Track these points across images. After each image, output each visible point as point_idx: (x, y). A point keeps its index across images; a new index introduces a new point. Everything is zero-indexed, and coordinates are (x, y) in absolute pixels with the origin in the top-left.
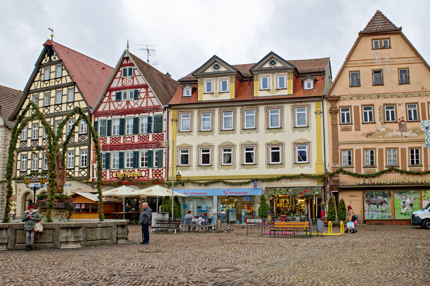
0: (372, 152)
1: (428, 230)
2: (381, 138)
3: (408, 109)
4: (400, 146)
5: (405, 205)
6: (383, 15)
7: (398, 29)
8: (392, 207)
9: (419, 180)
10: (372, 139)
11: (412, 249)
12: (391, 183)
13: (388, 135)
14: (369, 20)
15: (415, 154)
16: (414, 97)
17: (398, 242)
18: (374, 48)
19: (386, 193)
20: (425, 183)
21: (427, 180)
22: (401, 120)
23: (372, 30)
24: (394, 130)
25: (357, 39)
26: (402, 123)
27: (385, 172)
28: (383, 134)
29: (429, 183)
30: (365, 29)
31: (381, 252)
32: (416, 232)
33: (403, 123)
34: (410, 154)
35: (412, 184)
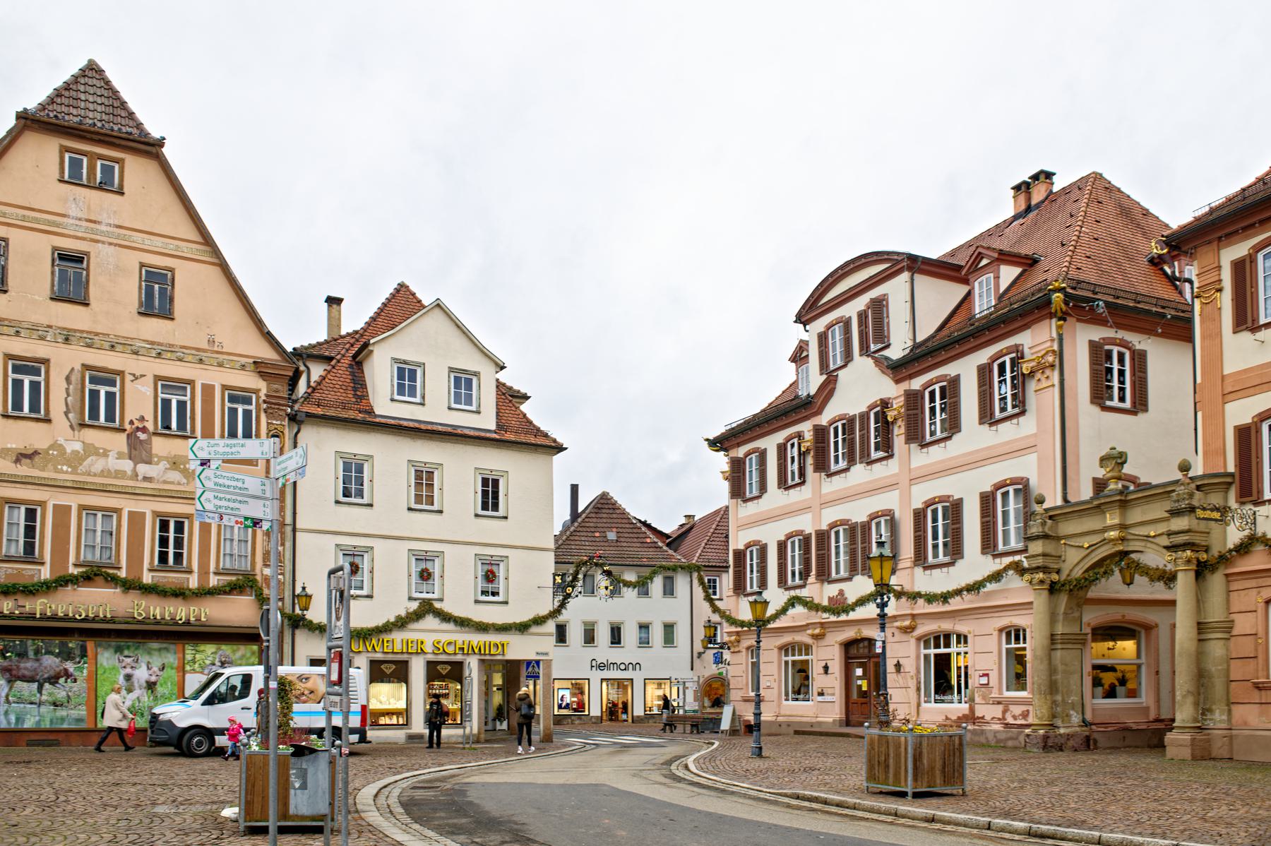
0: (31, 514)
1: (195, 760)
2: (67, 472)
3: (161, 396)
4: (128, 506)
5: (132, 685)
6: (108, 82)
7: (151, 141)
8: (89, 689)
9: (181, 611)
10: (36, 473)
11: (140, 816)
12: (91, 615)
13: (90, 466)
14: (59, 83)
15: (172, 535)
16: (183, 364)
17: (98, 796)
18: (66, 177)
19: (70, 645)
20: (198, 623)
21: (203, 615)
22: (137, 424)
23: (67, 118)
24: (110, 453)
25: (9, 132)
26: (139, 434)
27: (72, 581)
28: (75, 461)
29: (207, 624)
30: (43, 107)
31: (38, 830)
32: (159, 766)
33: (142, 436)
34: (158, 534)
35: (158, 623)
